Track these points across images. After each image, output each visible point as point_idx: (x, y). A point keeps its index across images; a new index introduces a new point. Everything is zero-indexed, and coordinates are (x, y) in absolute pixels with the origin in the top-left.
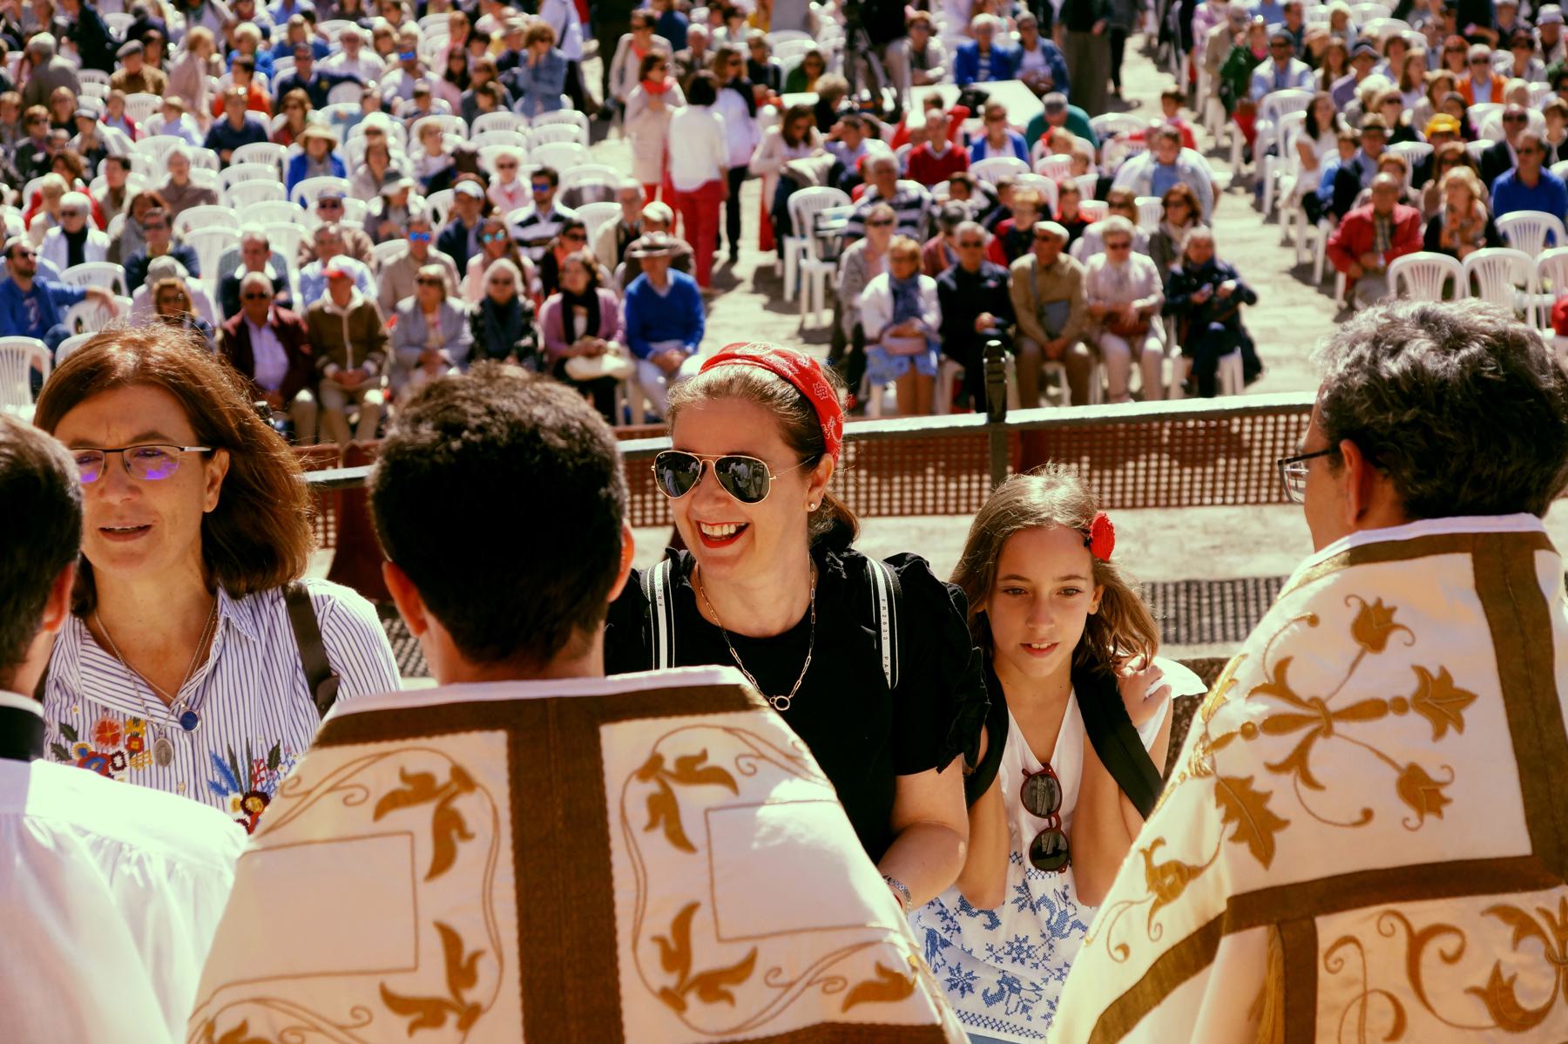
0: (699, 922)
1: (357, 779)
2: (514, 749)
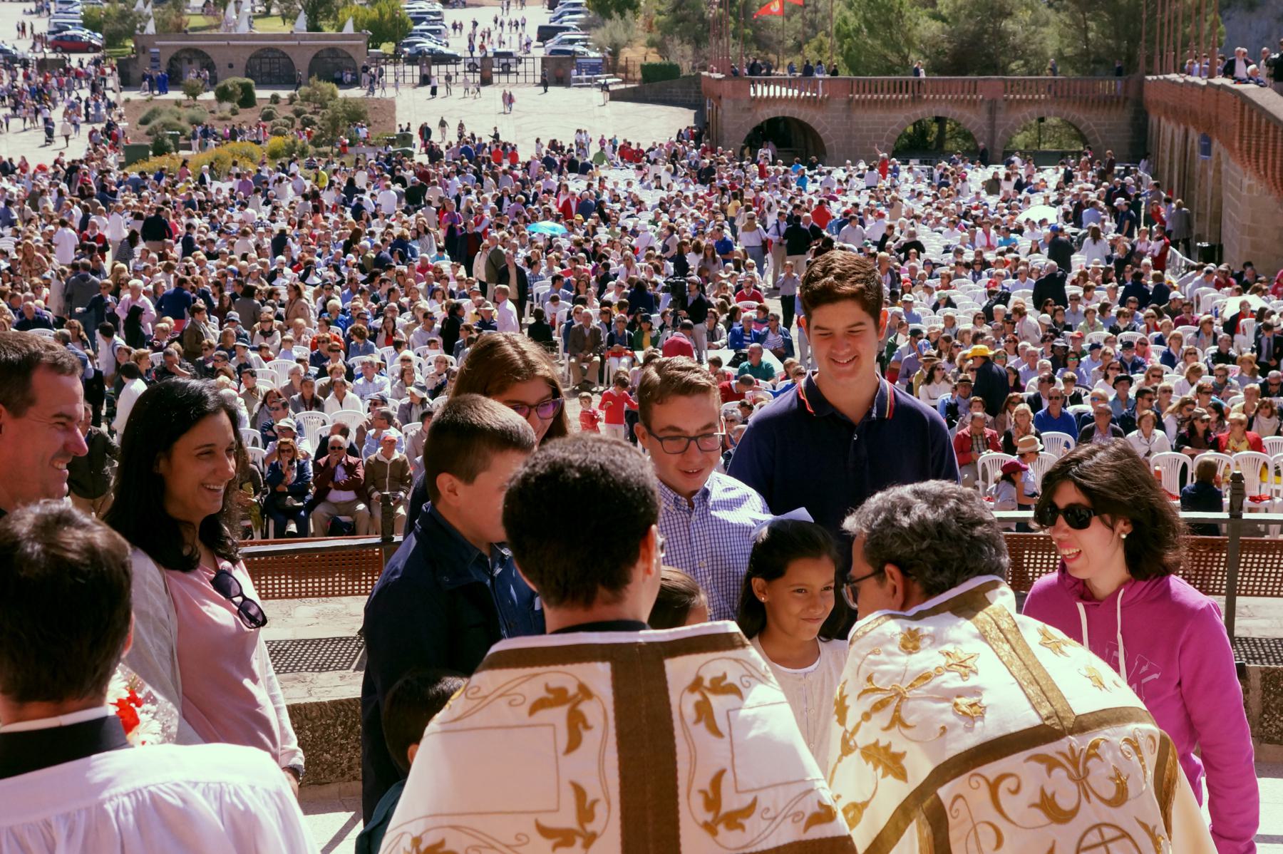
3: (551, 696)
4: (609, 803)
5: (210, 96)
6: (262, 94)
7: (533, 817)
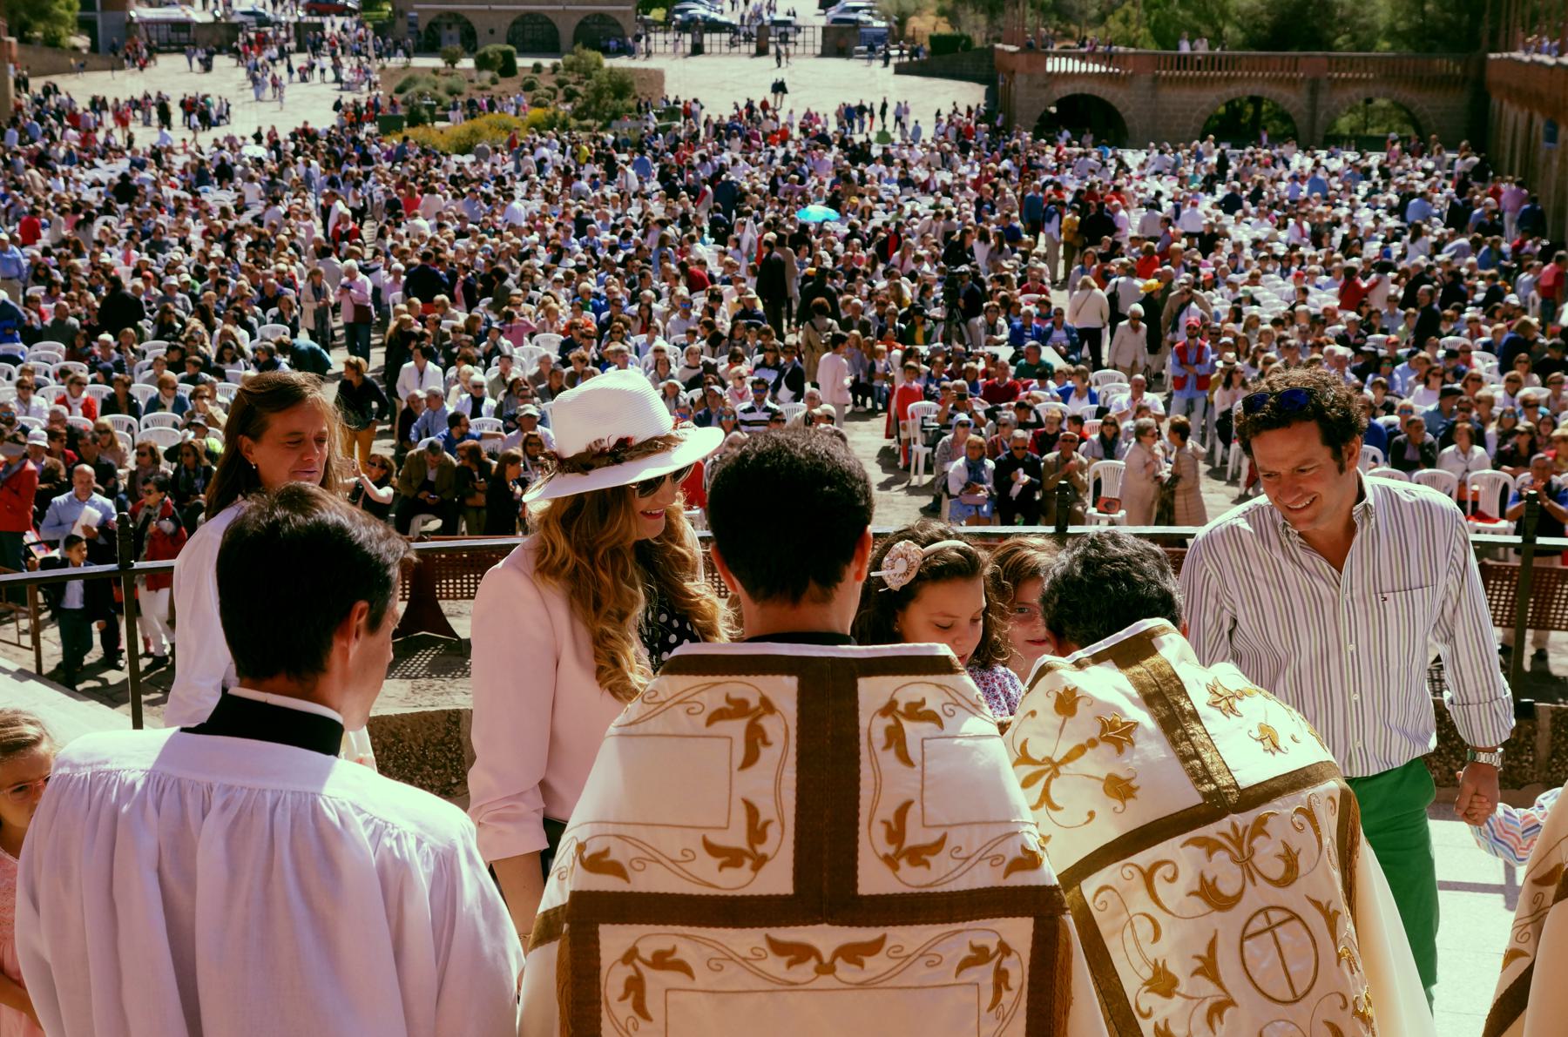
0: (913, 815)
1: (696, 698)
2: (801, 686)
3: (731, 707)
4: (783, 825)
5: (467, 63)
6: (524, 62)
7: (704, 832)
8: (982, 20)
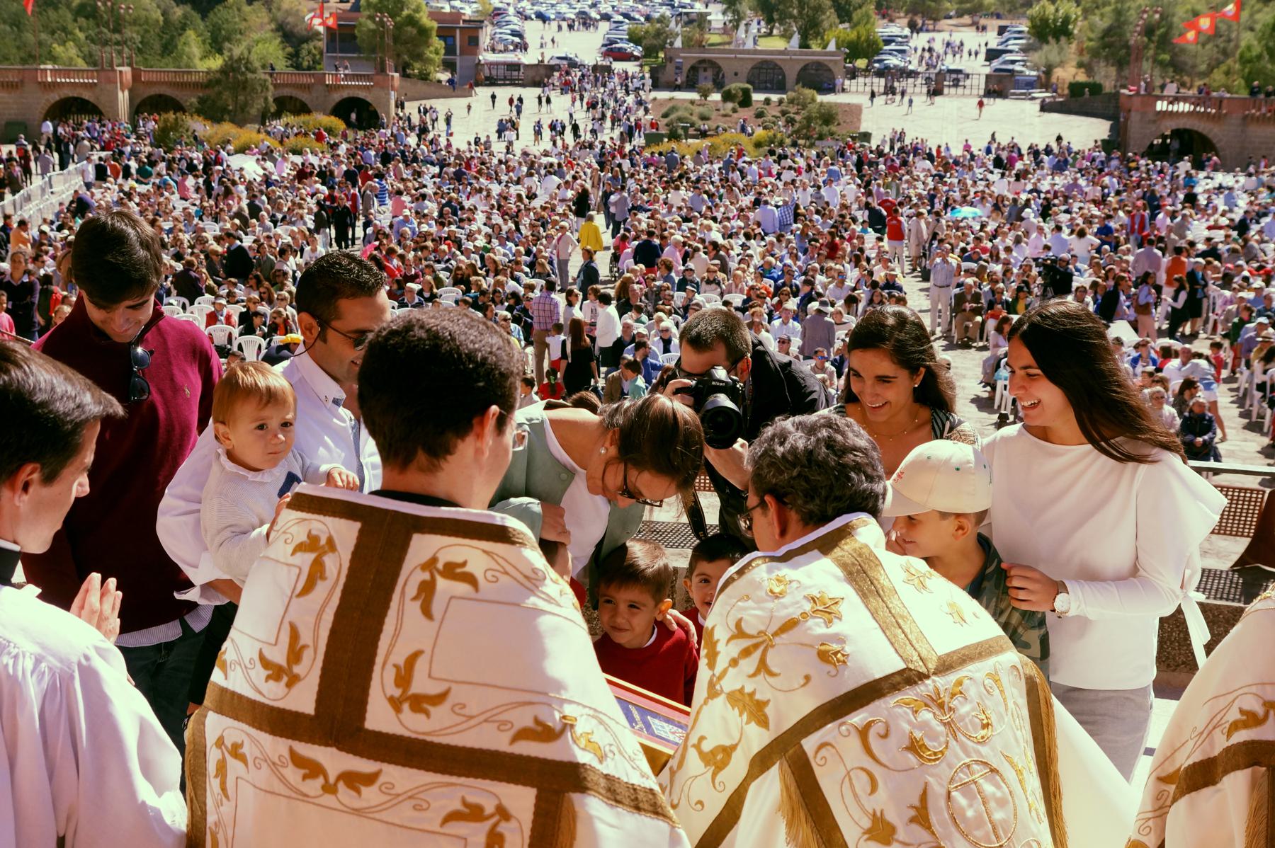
5: (716, 97)
6: (758, 97)
8: (1112, 71)
